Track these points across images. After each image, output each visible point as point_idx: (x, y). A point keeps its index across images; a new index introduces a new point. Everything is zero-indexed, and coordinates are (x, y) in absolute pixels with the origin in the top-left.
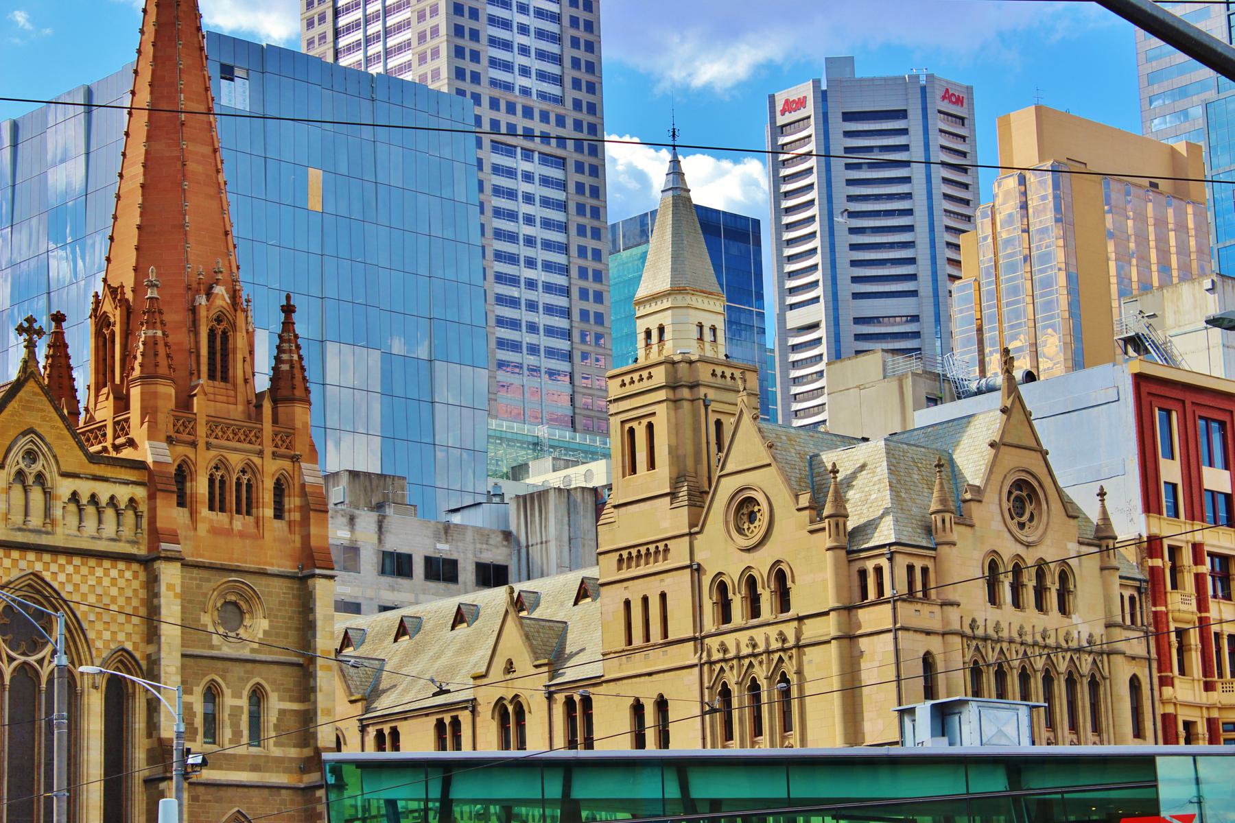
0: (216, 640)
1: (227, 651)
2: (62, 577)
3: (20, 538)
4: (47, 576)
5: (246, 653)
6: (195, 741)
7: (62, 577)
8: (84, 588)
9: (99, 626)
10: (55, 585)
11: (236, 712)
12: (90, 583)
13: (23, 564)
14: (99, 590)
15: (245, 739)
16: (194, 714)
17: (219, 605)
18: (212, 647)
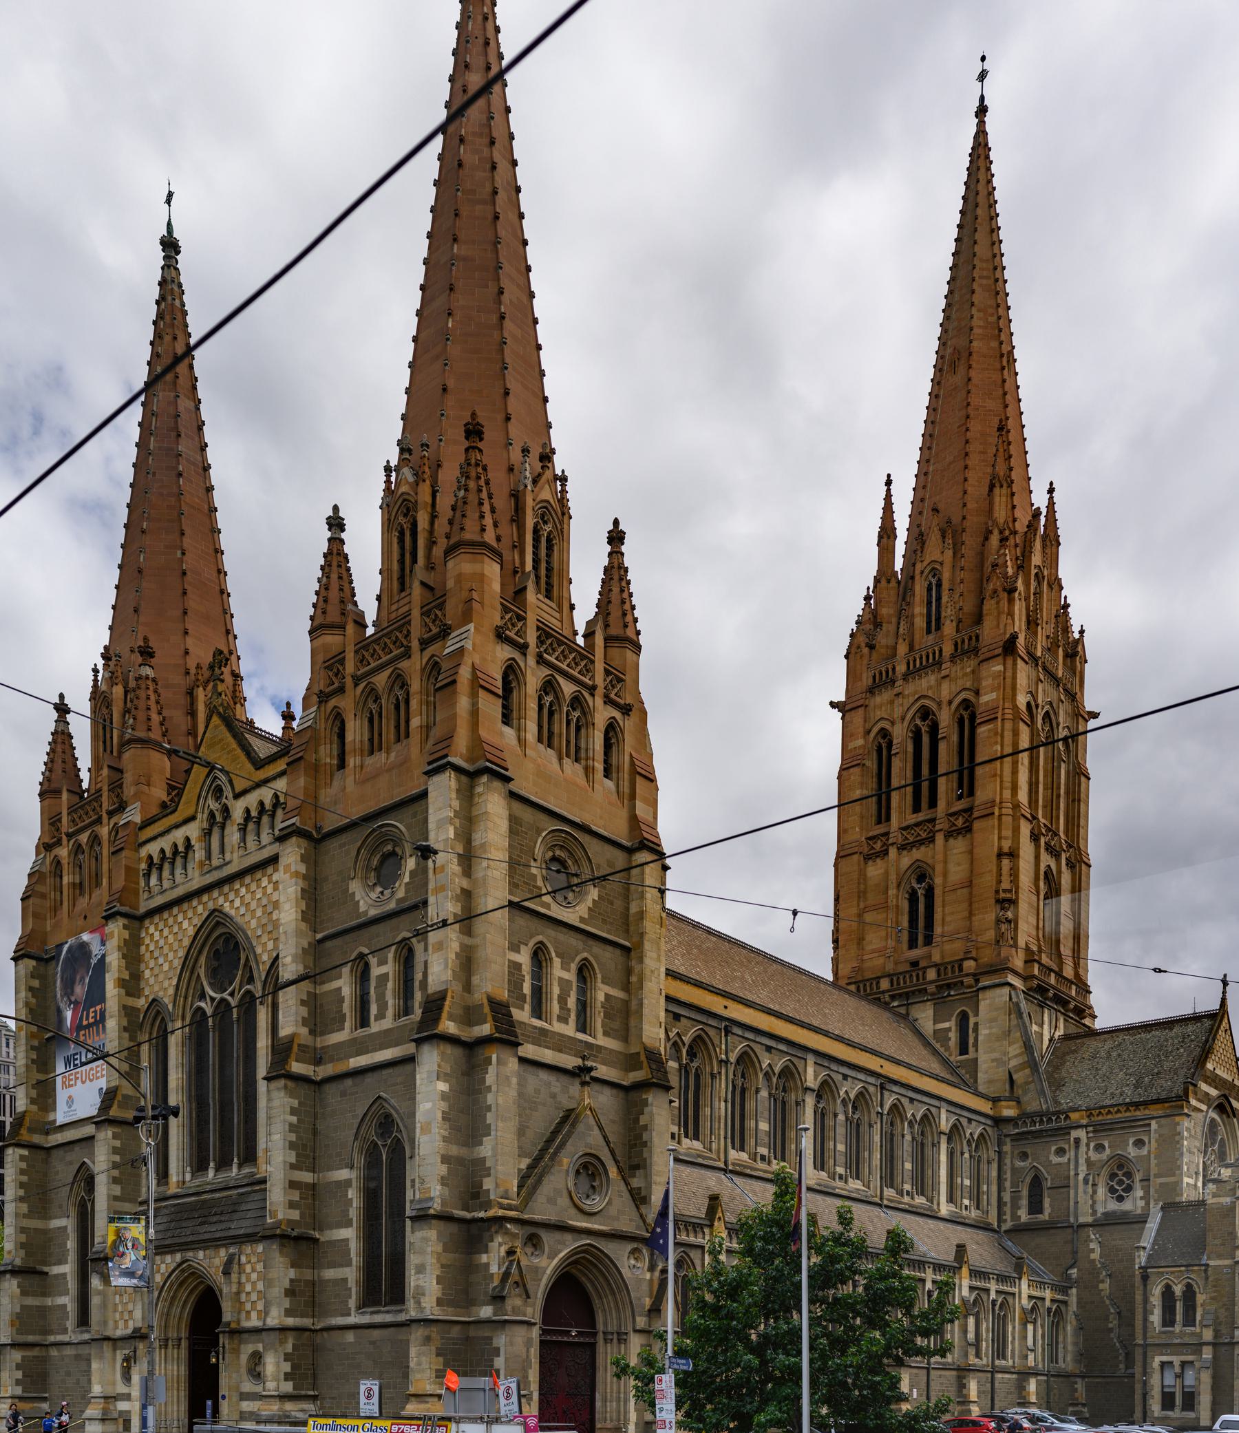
0: (363, 907)
1: (373, 912)
2: (237, 903)
3: (209, 879)
4: (227, 908)
5: (392, 905)
6: (343, 1029)
7: (237, 903)
8: (253, 905)
9: (264, 939)
10: (232, 912)
11: (383, 978)
12: (258, 896)
13: (211, 906)
14: (264, 902)
15: (390, 1012)
16: (342, 1000)
17: (375, 862)
18: (359, 916)
